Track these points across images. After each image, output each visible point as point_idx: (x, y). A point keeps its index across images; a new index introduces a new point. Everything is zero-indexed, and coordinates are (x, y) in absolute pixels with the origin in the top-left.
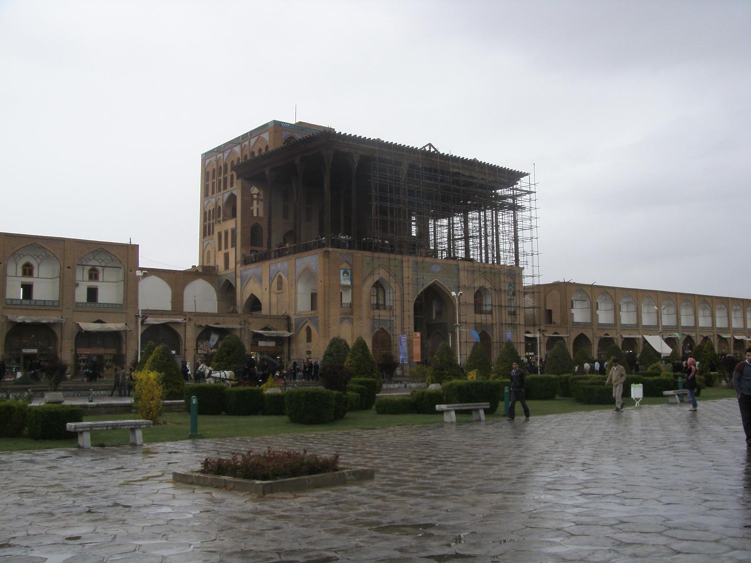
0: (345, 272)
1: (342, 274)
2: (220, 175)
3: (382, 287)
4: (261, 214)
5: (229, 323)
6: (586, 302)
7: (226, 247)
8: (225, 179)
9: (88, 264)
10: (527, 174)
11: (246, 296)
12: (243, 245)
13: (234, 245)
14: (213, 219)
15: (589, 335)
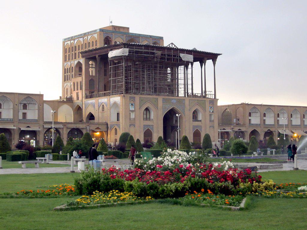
0: (132, 105)
1: (130, 105)
2: (73, 51)
3: (149, 110)
4: (94, 74)
5: (80, 126)
6: (258, 114)
7: (77, 90)
8: (75, 54)
9: (22, 103)
10: (221, 54)
11: (88, 113)
12: (86, 90)
13: (81, 89)
14: (69, 73)
15: (258, 130)
